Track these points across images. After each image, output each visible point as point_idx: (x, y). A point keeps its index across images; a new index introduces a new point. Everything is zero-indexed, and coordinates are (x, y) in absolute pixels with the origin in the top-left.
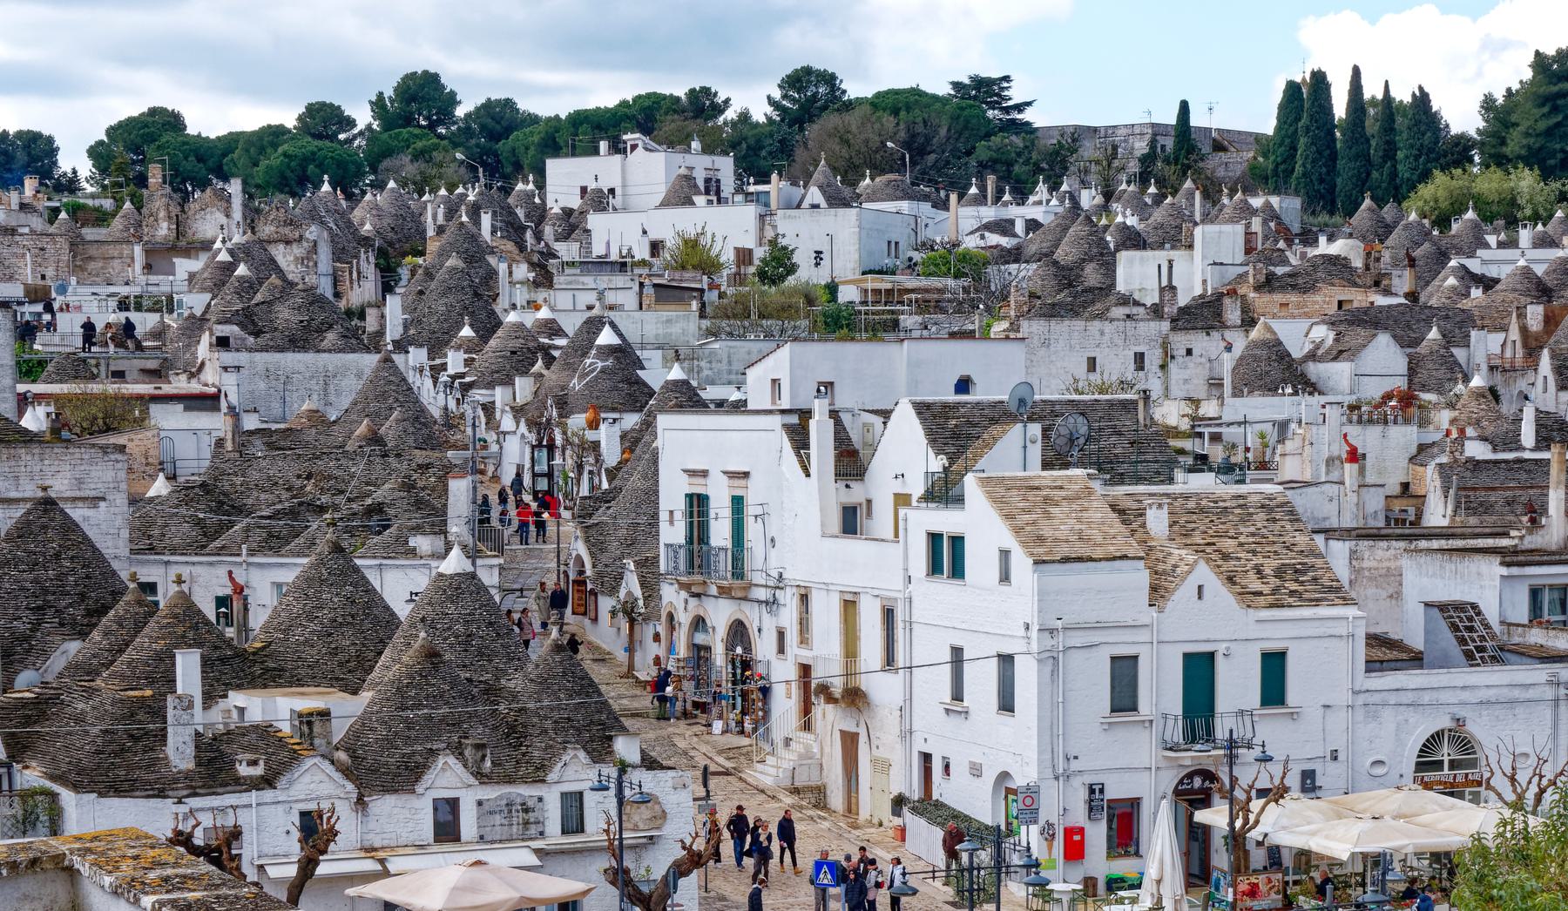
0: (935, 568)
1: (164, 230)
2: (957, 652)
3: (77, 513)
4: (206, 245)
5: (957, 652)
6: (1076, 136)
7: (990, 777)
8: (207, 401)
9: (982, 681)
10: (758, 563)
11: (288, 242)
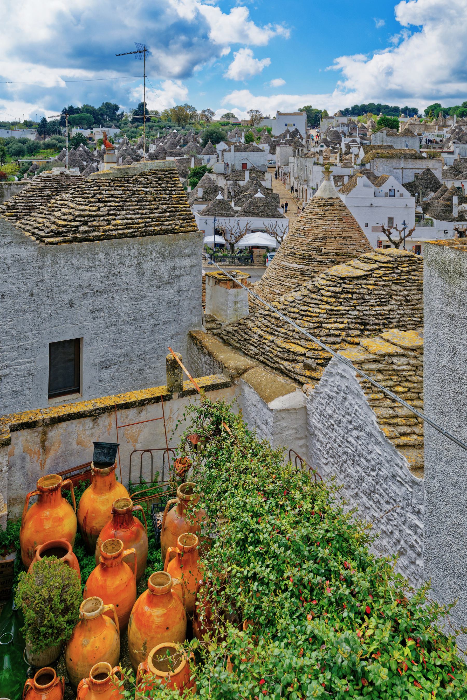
1: (441, 123)
3: (433, 171)
4: (450, 126)
8: (451, 153)
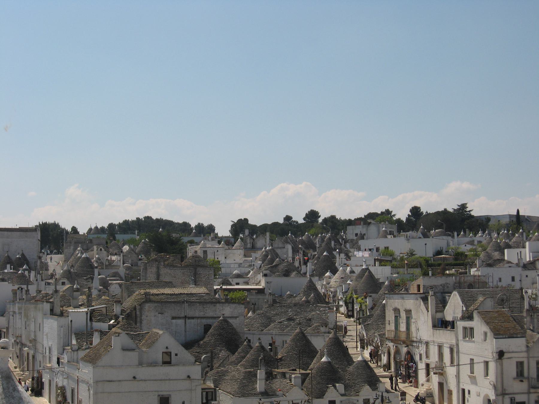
0: (465, 337)
1: (249, 246)
2: (472, 360)
5: (472, 360)
6: (488, 219)
7: (482, 396)
9: (479, 369)
10: (414, 335)
11: (280, 248)
